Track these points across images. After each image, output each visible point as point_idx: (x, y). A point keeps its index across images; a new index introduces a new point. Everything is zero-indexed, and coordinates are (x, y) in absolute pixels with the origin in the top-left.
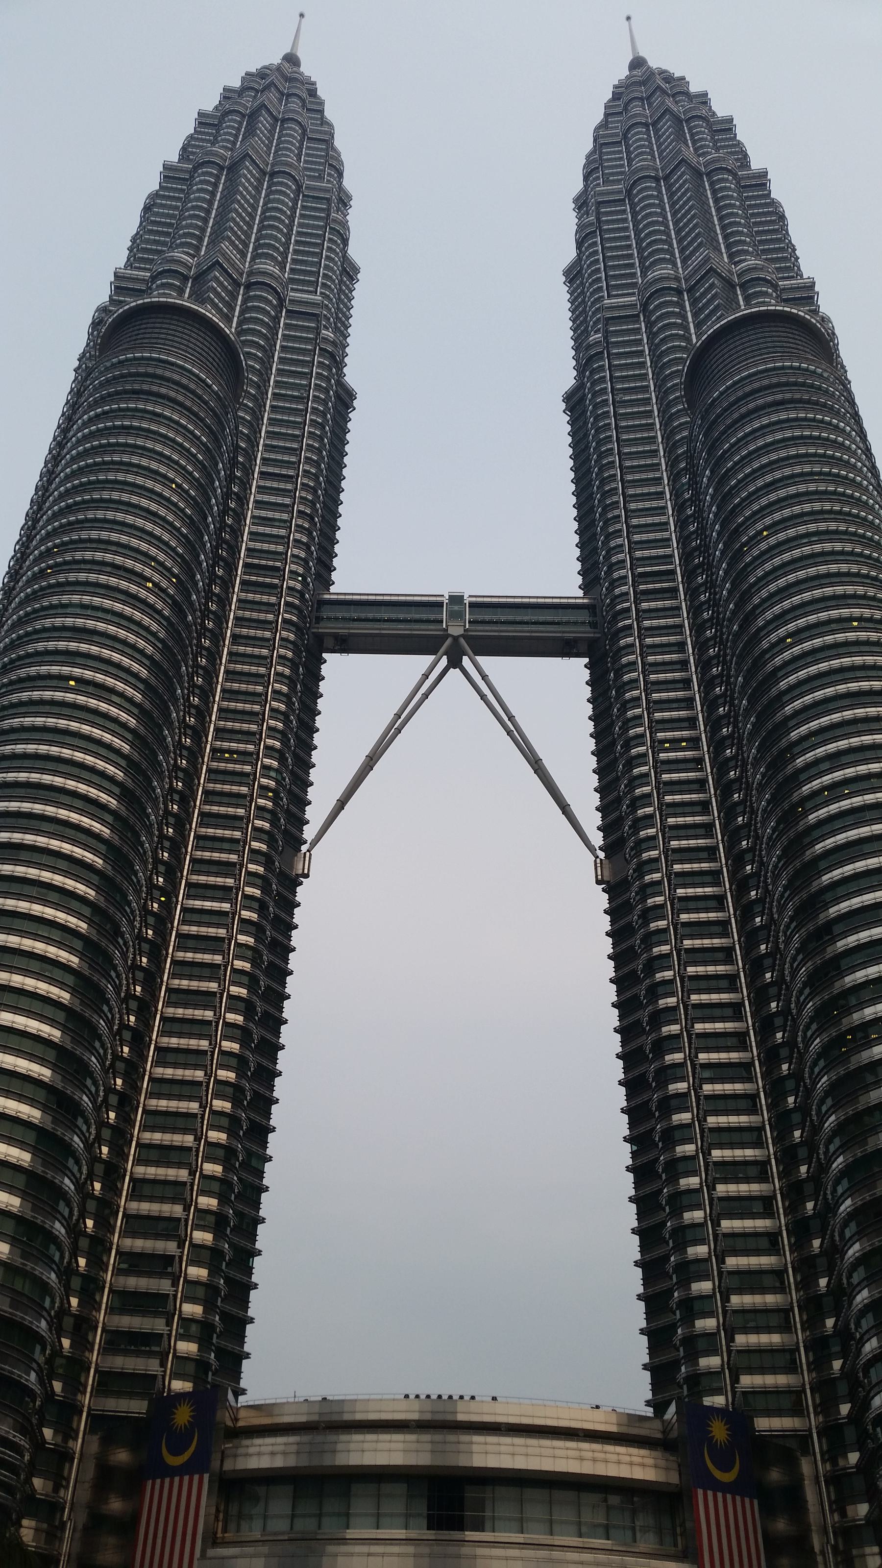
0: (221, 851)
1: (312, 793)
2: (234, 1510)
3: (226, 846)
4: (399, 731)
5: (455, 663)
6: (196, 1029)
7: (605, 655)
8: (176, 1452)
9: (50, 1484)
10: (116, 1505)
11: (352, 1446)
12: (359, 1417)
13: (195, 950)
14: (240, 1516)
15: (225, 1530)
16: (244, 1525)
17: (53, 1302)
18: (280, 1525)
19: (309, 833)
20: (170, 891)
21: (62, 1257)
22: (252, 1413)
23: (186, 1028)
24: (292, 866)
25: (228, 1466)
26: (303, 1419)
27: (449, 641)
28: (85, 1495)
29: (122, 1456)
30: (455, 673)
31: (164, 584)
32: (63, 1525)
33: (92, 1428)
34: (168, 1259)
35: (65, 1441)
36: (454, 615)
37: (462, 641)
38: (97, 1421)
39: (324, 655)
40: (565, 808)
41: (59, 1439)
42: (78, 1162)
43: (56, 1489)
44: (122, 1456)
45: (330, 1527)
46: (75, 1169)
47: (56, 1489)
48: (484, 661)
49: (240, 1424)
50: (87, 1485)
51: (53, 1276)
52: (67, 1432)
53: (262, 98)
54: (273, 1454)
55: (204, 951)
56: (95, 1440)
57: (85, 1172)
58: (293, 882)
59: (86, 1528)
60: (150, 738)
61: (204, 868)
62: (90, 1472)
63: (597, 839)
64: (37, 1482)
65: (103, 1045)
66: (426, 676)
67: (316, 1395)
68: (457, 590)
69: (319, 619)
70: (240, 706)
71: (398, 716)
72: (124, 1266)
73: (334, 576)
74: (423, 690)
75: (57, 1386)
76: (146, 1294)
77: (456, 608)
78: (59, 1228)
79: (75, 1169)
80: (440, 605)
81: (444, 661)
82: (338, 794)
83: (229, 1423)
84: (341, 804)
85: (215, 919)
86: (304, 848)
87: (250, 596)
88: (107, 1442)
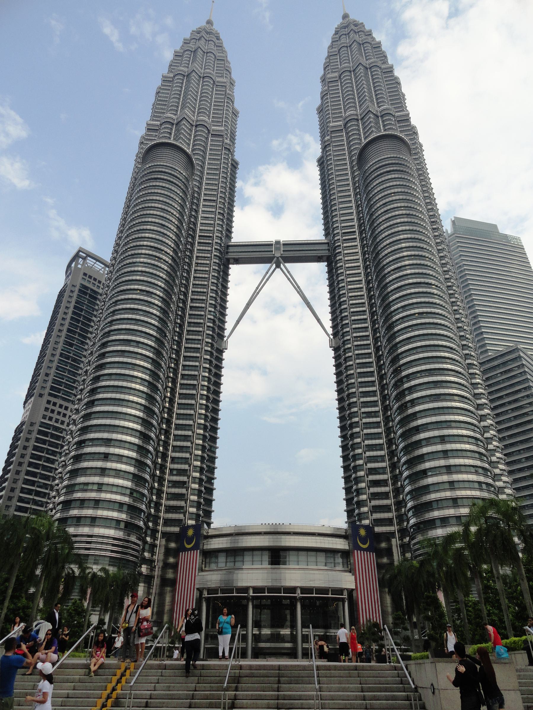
0: (195, 344)
1: (227, 319)
2: (208, 560)
3: (196, 342)
4: (258, 293)
8: (189, 544)
9: (150, 555)
10: (171, 560)
14: (210, 563)
15: (205, 567)
19: (227, 333)
24: (221, 346)
25: (205, 547)
27: (275, 259)
28: (161, 557)
29: (173, 545)
30: (278, 270)
32: (155, 566)
33: (163, 537)
34: (185, 483)
35: (154, 541)
36: (278, 249)
39: (230, 266)
41: (152, 541)
43: (152, 556)
44: (173, 545)
47: (152, 556)
52: (154, 538)
53: (198, 44)
55: (191, 380)
58: (221, 352)
62: (163, 550)
66: (267, 273)
68: (278, 239)
69: (227, 253)
71: (257, 288)
73: (233, 235)
75: (150, 524)
80: (272, 245)
81: (274, 266)
83: (205, 534)
84: (238, 322)
86: (225, 339)
88: (168, 541)
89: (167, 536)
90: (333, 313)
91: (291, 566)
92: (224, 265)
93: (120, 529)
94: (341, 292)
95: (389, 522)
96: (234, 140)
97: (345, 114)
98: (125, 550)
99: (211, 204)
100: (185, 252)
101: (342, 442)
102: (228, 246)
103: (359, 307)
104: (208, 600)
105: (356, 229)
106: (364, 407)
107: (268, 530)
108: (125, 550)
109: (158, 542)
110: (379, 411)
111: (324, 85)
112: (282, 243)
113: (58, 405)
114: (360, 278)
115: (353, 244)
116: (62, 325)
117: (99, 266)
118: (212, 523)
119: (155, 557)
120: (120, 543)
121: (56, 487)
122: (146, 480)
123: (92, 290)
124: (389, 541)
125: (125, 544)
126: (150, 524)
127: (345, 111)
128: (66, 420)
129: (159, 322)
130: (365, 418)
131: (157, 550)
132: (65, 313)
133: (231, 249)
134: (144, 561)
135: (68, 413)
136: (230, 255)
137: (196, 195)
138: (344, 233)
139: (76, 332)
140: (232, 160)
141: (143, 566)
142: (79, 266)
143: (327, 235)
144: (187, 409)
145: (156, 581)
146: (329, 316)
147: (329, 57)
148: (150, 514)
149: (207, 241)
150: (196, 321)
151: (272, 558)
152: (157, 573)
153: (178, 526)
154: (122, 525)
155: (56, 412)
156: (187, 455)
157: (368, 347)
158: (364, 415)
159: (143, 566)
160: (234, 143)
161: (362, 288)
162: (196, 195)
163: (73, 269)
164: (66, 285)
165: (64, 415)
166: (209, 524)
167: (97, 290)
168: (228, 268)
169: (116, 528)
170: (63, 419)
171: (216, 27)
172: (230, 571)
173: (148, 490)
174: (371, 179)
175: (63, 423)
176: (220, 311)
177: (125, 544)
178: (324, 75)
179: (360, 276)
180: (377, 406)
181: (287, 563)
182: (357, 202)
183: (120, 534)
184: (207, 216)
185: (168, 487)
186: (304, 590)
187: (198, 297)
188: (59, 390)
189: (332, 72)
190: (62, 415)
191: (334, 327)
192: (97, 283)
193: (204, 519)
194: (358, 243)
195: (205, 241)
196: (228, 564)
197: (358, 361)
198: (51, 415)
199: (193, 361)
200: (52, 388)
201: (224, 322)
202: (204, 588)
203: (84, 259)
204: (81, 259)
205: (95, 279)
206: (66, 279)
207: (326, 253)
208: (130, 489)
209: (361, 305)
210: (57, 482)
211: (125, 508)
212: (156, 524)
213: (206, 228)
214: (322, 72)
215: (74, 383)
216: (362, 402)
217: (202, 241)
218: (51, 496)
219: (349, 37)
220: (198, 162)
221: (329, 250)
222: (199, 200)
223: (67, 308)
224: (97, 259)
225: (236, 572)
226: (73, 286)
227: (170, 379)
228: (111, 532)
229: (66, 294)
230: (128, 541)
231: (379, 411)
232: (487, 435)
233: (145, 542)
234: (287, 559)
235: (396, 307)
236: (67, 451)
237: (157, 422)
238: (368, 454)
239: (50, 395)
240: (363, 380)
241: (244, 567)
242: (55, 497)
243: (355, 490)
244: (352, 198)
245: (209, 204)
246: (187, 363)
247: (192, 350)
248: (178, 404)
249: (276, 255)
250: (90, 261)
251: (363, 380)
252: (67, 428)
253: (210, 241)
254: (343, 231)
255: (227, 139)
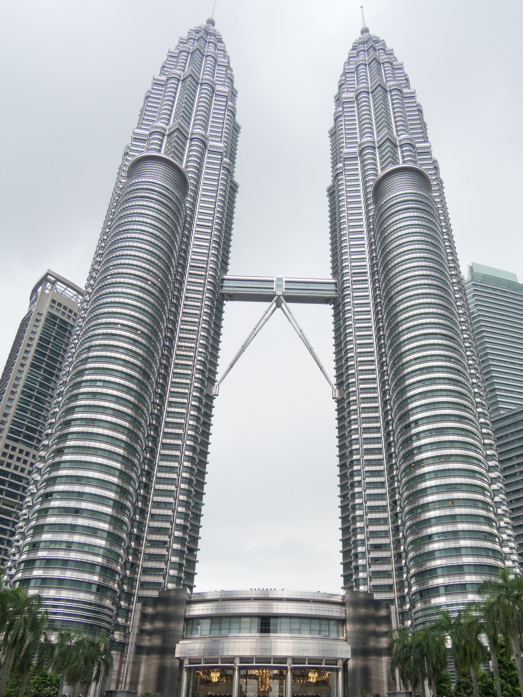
0: (182, 388)
1: (219, 361)
2: (190, 627)
3: (184, 386)
5: (278, 305)
6: (173, 459)
7: (339, 305)
11: (231, 607)
12: (234, 596)
13: (172, 428)
14: (192, 630)
16: (194, 632)
17: (125, 544)
18: (206, 633)
19: (218, 377)
20: (161, 405)
21: (128, 529)
22: (196, 595)
23: (169, 458)
26: (214, 597)
31: (156, 282)
32: (129, 633)
34: (165, 543)
35: (129, 604)
37: (282, 297)
38: (140, 599)
40: (321, 368)
41: (127, 605)
42: (132, 496)
43: (126, 621)
45: (224, 632)
46: (131, 499)
47: (126, 621)
48: (290, 305)
49: (192, 599)
50: (137, 620)
51: (125, 535)
52: (130, 603)
54: (203, 610)
55: (176, 428)
56: (140, 604)
57: (135, 499)
59: (137, 634)
60: (153, 337)
61: (175, 395)
62: (138, 616)
63: (334, 381)
64: (120, 620)
65: (139, 455)
67: (219, 590)
69: (222, 287)
70: (189, 327)
72: (148, 545)
74: (266, 317)
75: (125, 587)
76: (157, 555)
77: (280, 283)
78: (126, 519)
79: (131, 499)
80: (273, 281)
82: (230, 361)
83: (188, 599)
85: (179, 416)
86: (216, 384)
87: (193, 280)
88: (144, 605)
89: (145, 601)
90: (337, 361)
91: (282, 635)
92: (218, 300)
93: (91, 593)
94: (348, 339)
95: (389, 588)
96: (234, 158)
97: (361, 140)
98: (96, 616)
99: (206, 230)
100: (174, 284)
101: (342, 502)
102: (223, 280)
103: (368, 356)
104: (189, 669)
105: (368, 270)
106: (368, 465)
107: (259, 596)
108: (96, 616)
109: (133, 607)
110: (384, 471)
111: (337, 106)
112: (284, 280)
113: (17, 450)
114: (370, 325)
115: (364, 286)
116: (24, 358)
117: (70, 293)
118: (195, 586)
119: (130, 623)
120: (92, 608)
121: (16, 544)
122: (122, 540)
123: (61, 320)
124: (388, 607)
125: (97, 609)
126: (125, 587)
127: (361, 137)
128: (27, 467)
129: (142, 362)
130: (369, 477)
131: (132, 615)
132: (29, 345)
133: (226, 283)
134: (118, 627)
135: (30, 459)
136: (225, 290)
137: (188, 219)
138: (354, 273)
139: (41, 367)
140: (232, 181)
141: (116, 632)
142: (47, 291)
143: (335, 274)
144: (171, 461)
145: (131, 649)
146: (334, 364)
147: (345, 74)
148: (125, 576)
149: (200, 273)
150: (184, 362)
151: (261, 626)
152: (132, 640)
153: (157, 589)
154: (94, 588)
155: (15, 458)
156: (170, 512)
157: (376, 400)
158: (368, 474)
159: (116, 632)
160: (234, 163)
161: (371, 327)
162: (188, 219)
163: (39, 294)
164: (30, 313)
165: (25, 462)
166: (191, 588)
167: (67, 320)
168: (223, 305)
169: (86, 592)
170: (24, 466)
171: (218, 28)
172: (215, 640)
173: (124, 550)
174: (387, 215)
175: (23, 470)
176: (211, 353)
177: (97, 609)
178: (339, 93)
179: (370, 322)
180: (382, 464)
181: (278, 631)
182: (370, 240)
183: (90, 598)
184: (201, 243)
185: (146, 547)
186: (295, 660)
187: (188, 336)
188: (19, 433)
189: (348, 92)
190: (22, 461)
191: (338, 377)
192: (67, 312)
193: (186, 583)
194: (369, 285)
195: (197, 272)
196: (213, 632)
197: (363, 415)
198: (10, 461)
199: (179, 407)
200: (12, 431)
201: (215, 365)
202: (185, 658)
203: (53, 283)
204: (49, 284)
205: (65, 308)
206: (30, 306)
207: (333, 294)
208: (104, 548)
209: (369, 354)
210: (17, 537)
211: (98, 569)
212: (132, 587)
213: (199, 258)
214: (336, 91)
215: (37, 425)
216: (365, 460)
217: (194, 272)
218: (9, 554)
219: (368, 55)
220: (192, 181)
221: (336, 291)
222: (191, 224)
223: (31, 339)
224: (69, 285)
225: (222, 640)
226: (39, 314)
227: (152, 427)
228: (82, 596)
229: (30, 322)
230: (100, 606)
231: (384, 471)
232: (497, 499)
233: (119, 607)
234: (278, 628)
235: (408, 359)
236: (31, 504)
237: (137, 475)
238: (370, 516)
239: (9, 438)
240: (368, 436)
241: (230, 635)
242: (14, 555)
243: (354, 554)
244: (365, 235)
245: (203, 230)
246: (173, 410)
247: (179, 395)
248: (160, 455)
249: (277, 293)
250: (60, 286)
251: (368, 436)
252: (28, 477)
253: (203, 273)
254: (354, 271)
255: (226, 157)
